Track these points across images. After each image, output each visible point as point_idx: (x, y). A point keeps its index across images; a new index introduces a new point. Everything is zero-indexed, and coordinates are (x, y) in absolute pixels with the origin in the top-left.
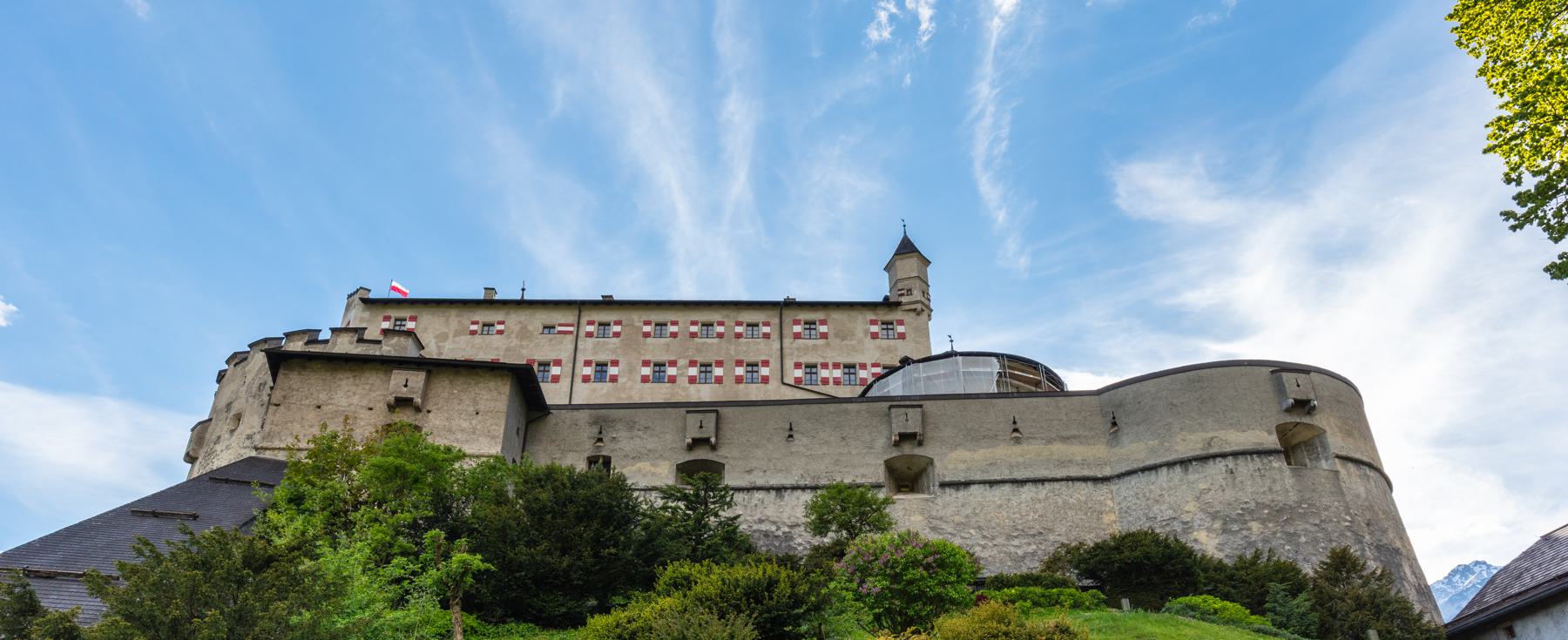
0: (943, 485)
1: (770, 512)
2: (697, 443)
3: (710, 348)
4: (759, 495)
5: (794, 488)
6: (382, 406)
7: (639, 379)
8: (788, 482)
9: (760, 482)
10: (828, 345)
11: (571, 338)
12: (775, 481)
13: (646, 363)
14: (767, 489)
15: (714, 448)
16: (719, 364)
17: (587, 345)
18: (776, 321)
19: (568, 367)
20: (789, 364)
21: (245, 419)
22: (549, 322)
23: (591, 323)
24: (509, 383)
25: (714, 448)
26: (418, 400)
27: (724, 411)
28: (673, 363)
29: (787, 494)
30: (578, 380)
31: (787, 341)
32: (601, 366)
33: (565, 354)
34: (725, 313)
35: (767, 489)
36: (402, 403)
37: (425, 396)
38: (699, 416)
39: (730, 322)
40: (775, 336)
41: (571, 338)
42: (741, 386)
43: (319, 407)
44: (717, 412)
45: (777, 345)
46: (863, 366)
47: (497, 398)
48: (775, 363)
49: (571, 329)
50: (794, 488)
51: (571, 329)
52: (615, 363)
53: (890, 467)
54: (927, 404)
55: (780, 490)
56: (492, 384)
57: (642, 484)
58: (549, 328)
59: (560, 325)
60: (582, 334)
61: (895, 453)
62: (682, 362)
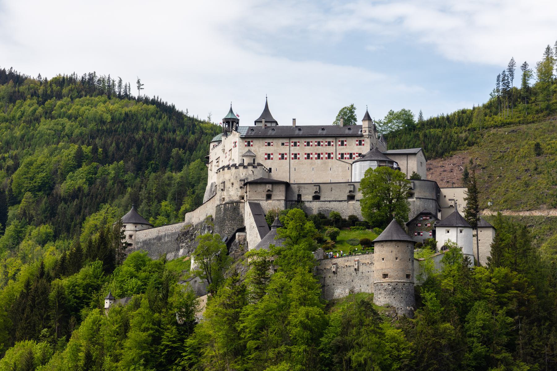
0: (357, 201)
1: (328, 206)
2: (316, 192)
3: (320, 150)
4: (326, 202)
5: (332, 201)
6: (265, 191)
8: (331, 200)
9: (326, 200)
10: (346, 148)
11: (288, 147)
12: (329, 200)
13: (306, 154)
14: (328, 201)
15: (319, 193)
16: (322, 154)
17: (292, 148)
18: (334, 141)
19: (288, 155)
20: (338, 154)
22: (283, 142)
23: (292, 142)
25: (319, 193)
27: (321, 185)
28: (312, 154)
29: (331, 202)
30: (291, 159)
31: (337, 146)
32: (296, 155)
33: (287, 152)
34: (323, 138)
35: (328, 201)
36: (269, 190)
38: (316, 187)
39: (324, 141)
40: (334, 145)
41: (288, 147)
44: (319, 186)
45: (335, 148)
46: (354, 154)
47: (283, 188)
48: (334, 154)
50: (332, 201)
52: (299, 154)
53: (348, 196)
54: (355, 184)
55: (330, 201)
56: (282, 185)
57: (307, 200)
58: (283, 144)
61: (349, 194)
62: (314, 153)
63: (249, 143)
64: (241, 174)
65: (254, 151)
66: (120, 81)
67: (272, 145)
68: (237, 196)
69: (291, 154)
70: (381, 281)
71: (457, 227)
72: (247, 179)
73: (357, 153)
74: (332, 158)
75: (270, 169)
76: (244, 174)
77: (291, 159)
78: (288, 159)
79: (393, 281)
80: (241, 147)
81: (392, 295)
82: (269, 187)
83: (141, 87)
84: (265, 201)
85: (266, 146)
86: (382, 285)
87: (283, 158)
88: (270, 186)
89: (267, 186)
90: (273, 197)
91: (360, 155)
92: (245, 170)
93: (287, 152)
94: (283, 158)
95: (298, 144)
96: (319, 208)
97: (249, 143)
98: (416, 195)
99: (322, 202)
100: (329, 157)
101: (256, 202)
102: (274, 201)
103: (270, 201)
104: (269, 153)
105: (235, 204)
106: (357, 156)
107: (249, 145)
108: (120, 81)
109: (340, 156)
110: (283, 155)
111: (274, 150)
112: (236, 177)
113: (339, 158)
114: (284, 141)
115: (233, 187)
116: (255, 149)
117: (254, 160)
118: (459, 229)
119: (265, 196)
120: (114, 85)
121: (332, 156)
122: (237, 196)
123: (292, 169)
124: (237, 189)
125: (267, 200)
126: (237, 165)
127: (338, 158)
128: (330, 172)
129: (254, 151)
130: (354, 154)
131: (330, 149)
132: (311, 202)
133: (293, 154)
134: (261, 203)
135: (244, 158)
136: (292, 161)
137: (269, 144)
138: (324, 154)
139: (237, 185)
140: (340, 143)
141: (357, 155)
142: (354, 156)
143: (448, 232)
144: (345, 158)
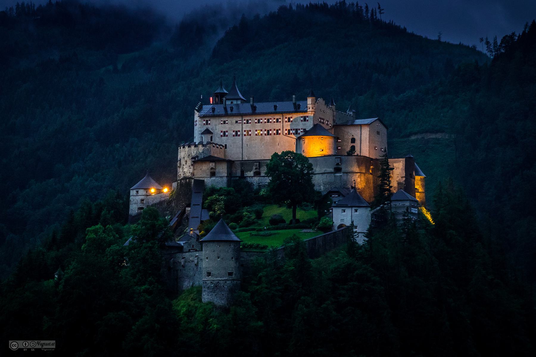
7: (255, 135)
11: (241, 124)
17: (244, 126)
18: (282, 118)
19: (241, 132)
20: (284, 130)
21: (188, 162)
23: (245, 120)
24: (226, 164)
26: (214, 168)
30: (243, 135)
31: (284, 123)
33: (240, 130)
36: (212, 168)
37: (215, 167)
40: (282, 122)
42: (275, 135)
43: (201, 169)
45: (282, 125)
46: (299, 130)
48: (281, 129)
49: (241, 122)
51: (241, 122)
58: (237, 122)
59: (239, 121)
60: (243, 123)
63: (207, 121)
64: (193, 153)
65: (212, 129)
66: (367, 7)
67: (227, 123)
68: (190, 173)
69: (243, 131)
70: (206, 279)
71: (352, 207)
72: (197, 157)
73: (301, 129)
74: (280, 134)
75: (226, 145)
76: (195, 152)
77: (243, 135)
78: (241, 136)
79: (215, 279)
80: (200, 126)
81: (214, 292)
82: (212, 165)
83: (382, 12)
84: (209, 178)
85: (222, 124)
86: (206, 283)
87: (237, 135)
88: (214, 164)
89: (211, 164)
90: (217, 175)
91: (305, 130)
92: (196, 148)
93: (240, 130)
94: (237, 135)
95: (250, 121)
96: (259, 183)
97: (207, 121)
98: (343, 170)
99: (262, 178)
100: (278, 133)
101: (201, 179)
102: (217, 178)
103: (213, 178)
104: (224, 130)
105: (188, 180)
106: (302, 132)
107: (207, 123)
108: (367, 7)
109: (286, 132)
110: (237, 132)
111: (229, 128)
112: (189, 155)
113: (286, 134)
114: (239, 119)
115: (186, 164)
116: (212, 127)
117: (211, 137)
118: (353, 209)
119: (209, 174)
120: (362, 10)
121: (280, 132)
122: (190, 173)
123: (245, 145)
124: (189, 166)
125: (211, 177)
126: (197, 144)
127: (284, 134)
128: (279, 147)
129: (212, 129)
130: (299, 130)
131: (278, 126)
132: (252, 177)
133: (245, 131)
134: (206, 180)
135: (203, 136)
136: (244, 137)
137: (224, 122)
138: (273, 130)
139: (189, 163)
140: (286, 120)
141: (302, 130)
142: (299, 132)
143: (344, 212)
144: (291, 134)
